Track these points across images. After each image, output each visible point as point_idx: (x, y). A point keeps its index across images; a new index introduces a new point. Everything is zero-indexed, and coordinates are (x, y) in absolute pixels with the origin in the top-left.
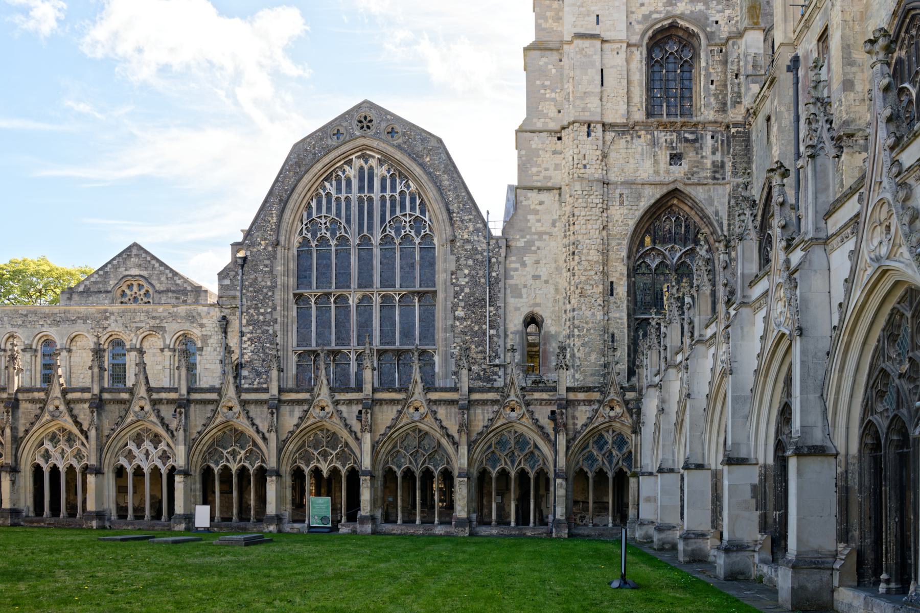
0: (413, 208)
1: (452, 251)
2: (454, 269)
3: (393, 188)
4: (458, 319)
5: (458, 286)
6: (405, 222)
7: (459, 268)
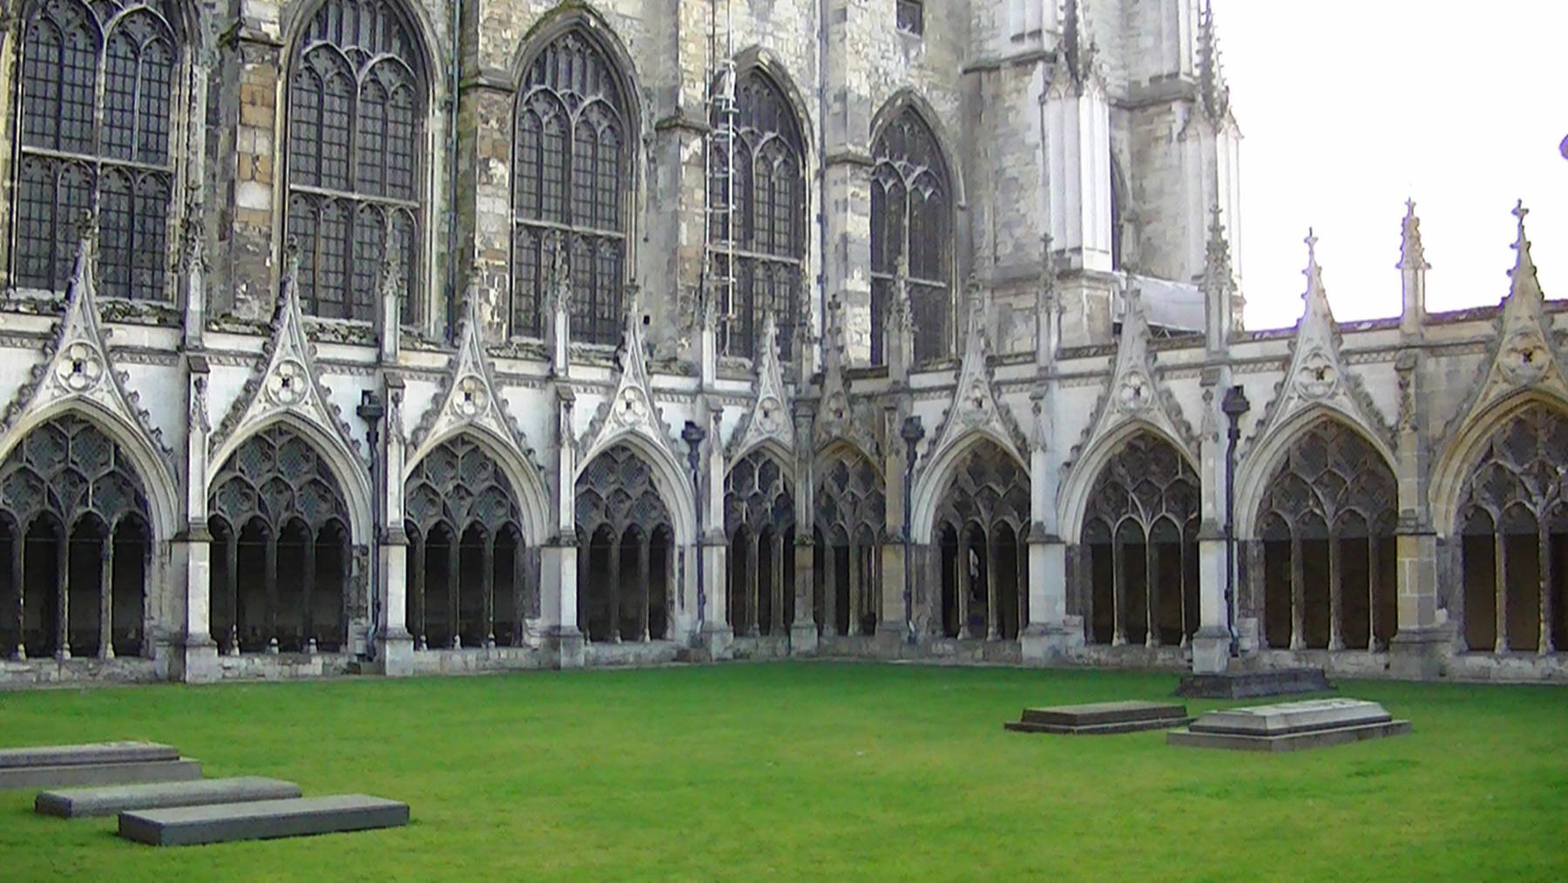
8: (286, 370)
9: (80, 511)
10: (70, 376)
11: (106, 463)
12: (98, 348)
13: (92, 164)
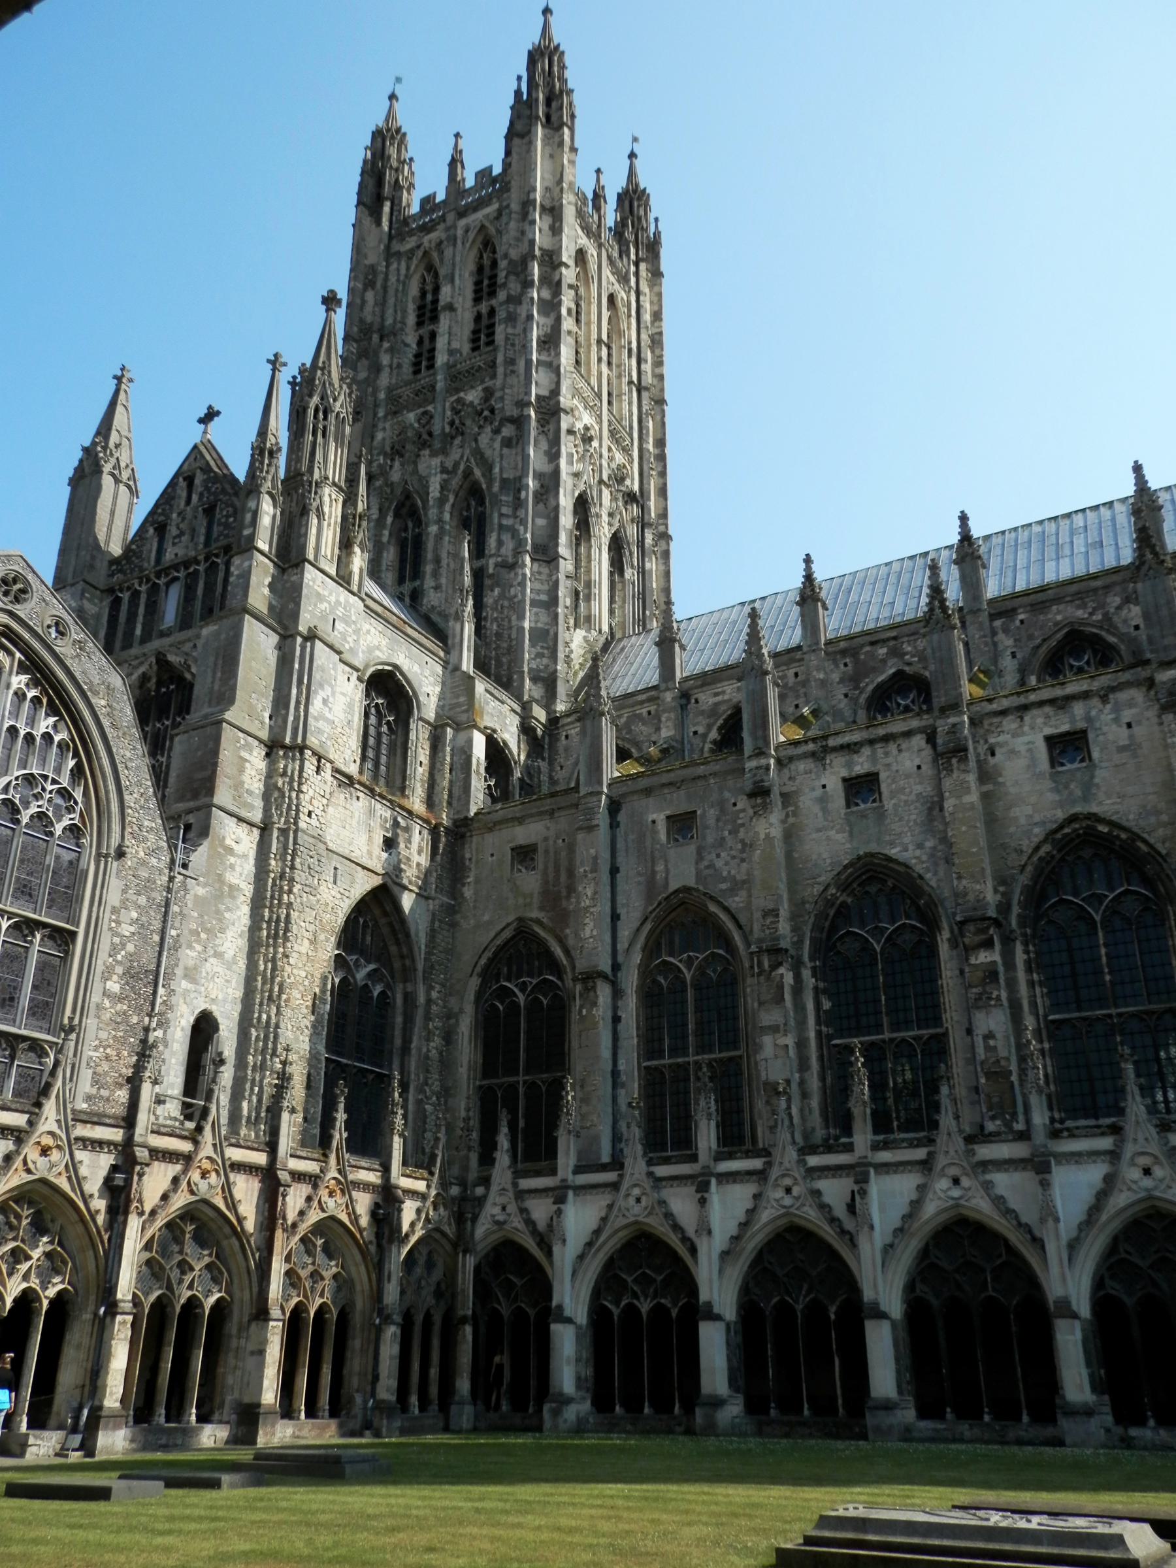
0: (58, 770)
1: (119, 872)
2: (117, 904)
3: (32, 722)
4: (109, 996)
5: (118, 935)
6: (44, 789)
7: (124, 904)
8: (1144, 1161)
9: (983, 1295)
10: (949, 1189)
11: (1000, 1256)
12: (965, 1164)
13: (1110, 1016)
